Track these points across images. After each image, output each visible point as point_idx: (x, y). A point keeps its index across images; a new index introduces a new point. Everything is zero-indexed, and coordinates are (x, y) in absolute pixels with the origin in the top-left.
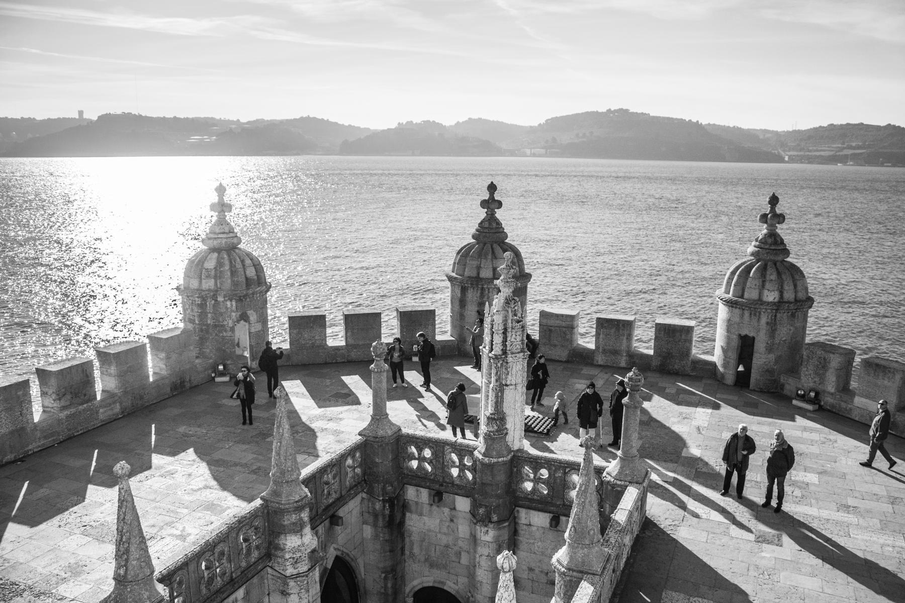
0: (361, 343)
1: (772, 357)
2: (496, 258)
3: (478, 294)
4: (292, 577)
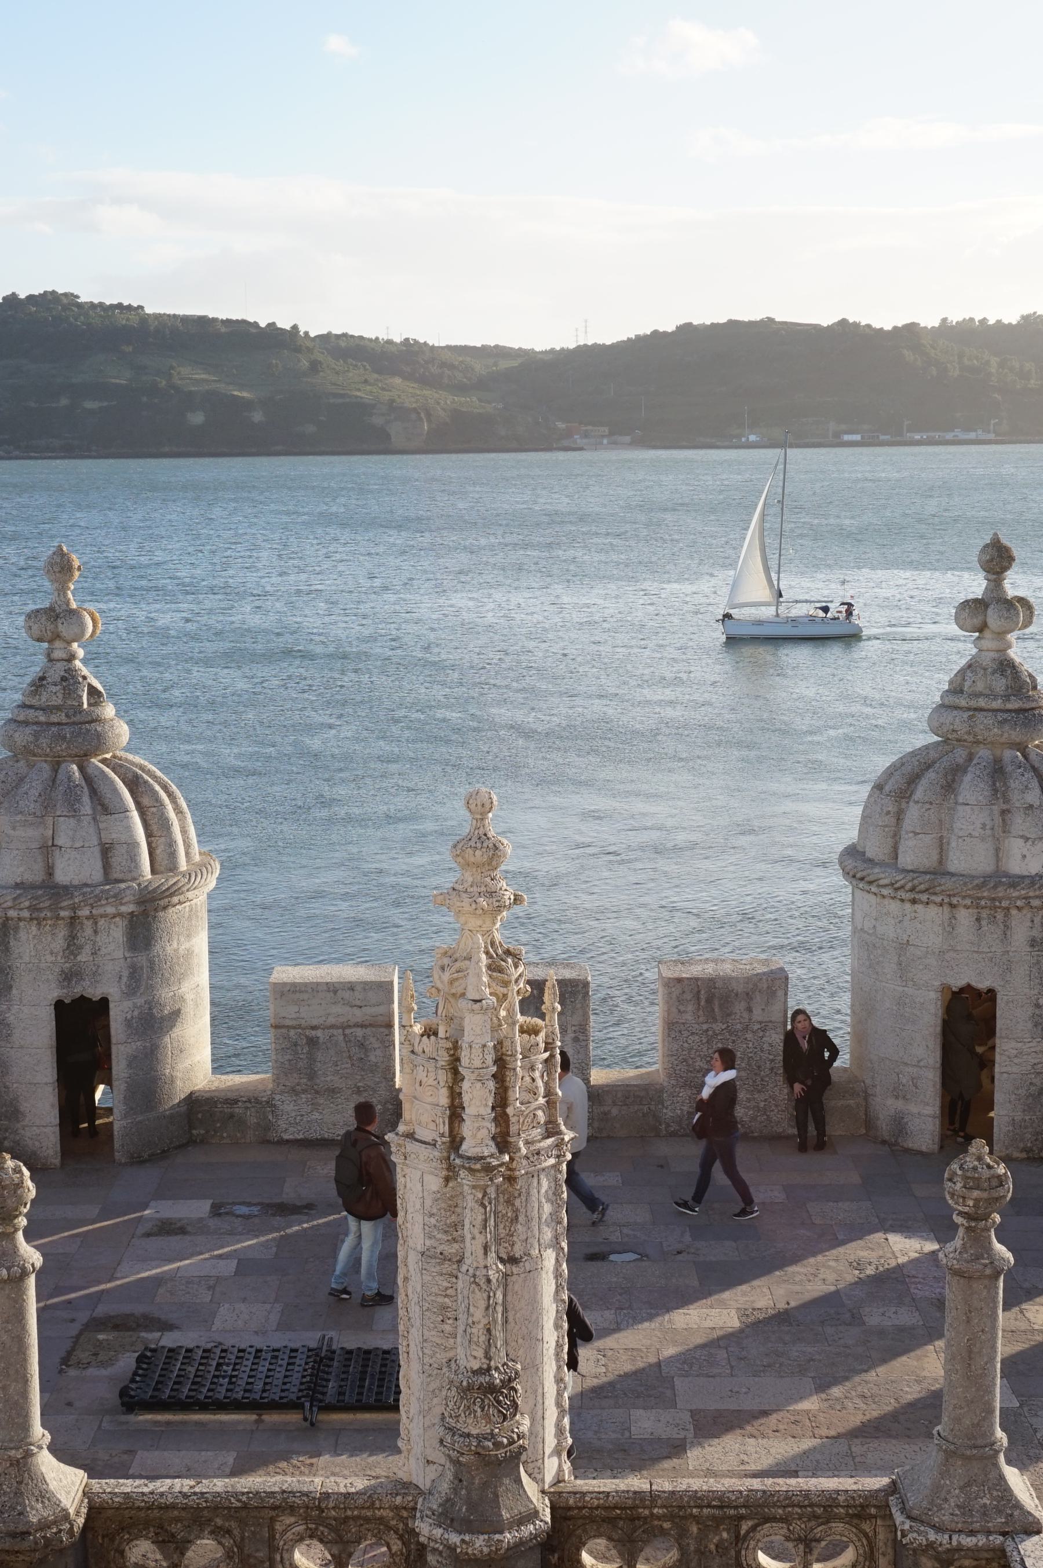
2: (106, 810)
3: (59, 942)
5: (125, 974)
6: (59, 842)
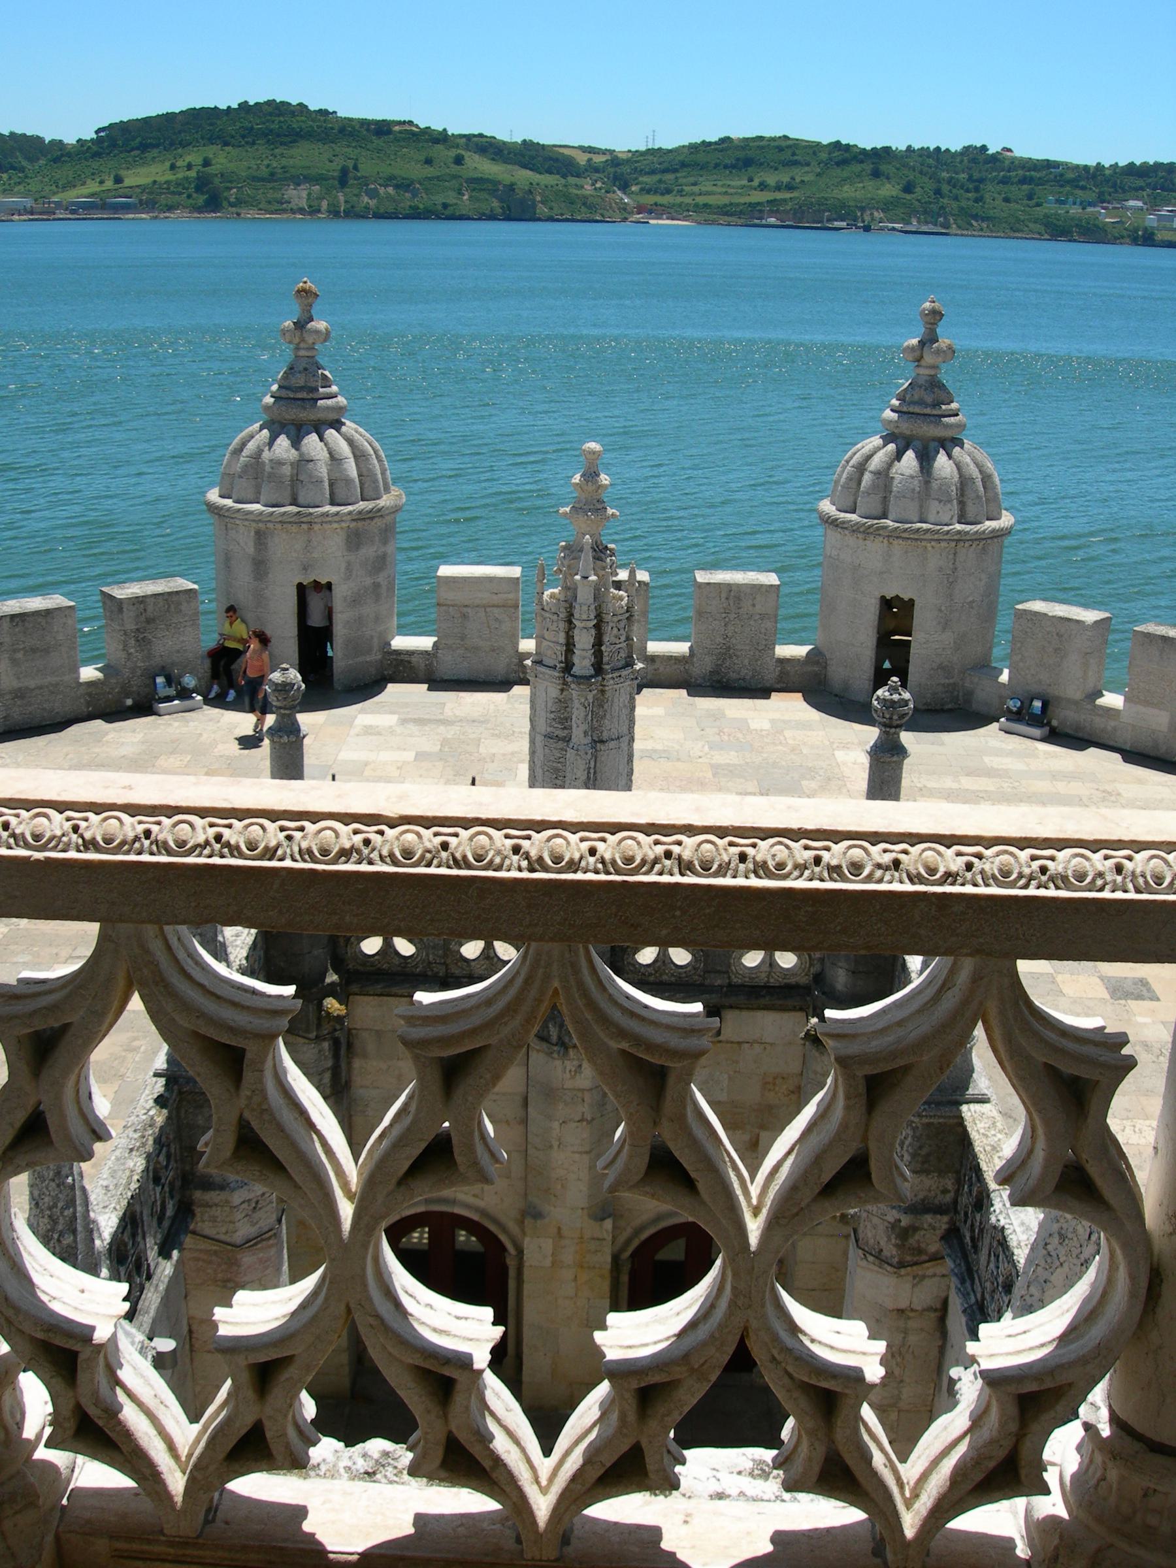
0: (32, 684)
1: (948, 638)
4: (252, 1242)
5: (343, 566)
6: (301, 478)
